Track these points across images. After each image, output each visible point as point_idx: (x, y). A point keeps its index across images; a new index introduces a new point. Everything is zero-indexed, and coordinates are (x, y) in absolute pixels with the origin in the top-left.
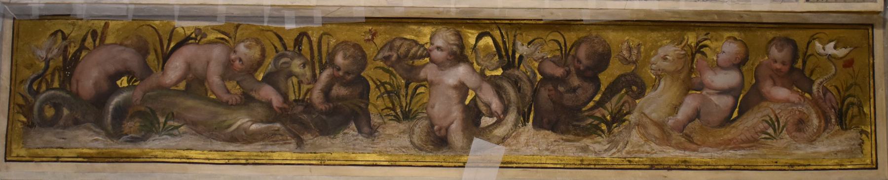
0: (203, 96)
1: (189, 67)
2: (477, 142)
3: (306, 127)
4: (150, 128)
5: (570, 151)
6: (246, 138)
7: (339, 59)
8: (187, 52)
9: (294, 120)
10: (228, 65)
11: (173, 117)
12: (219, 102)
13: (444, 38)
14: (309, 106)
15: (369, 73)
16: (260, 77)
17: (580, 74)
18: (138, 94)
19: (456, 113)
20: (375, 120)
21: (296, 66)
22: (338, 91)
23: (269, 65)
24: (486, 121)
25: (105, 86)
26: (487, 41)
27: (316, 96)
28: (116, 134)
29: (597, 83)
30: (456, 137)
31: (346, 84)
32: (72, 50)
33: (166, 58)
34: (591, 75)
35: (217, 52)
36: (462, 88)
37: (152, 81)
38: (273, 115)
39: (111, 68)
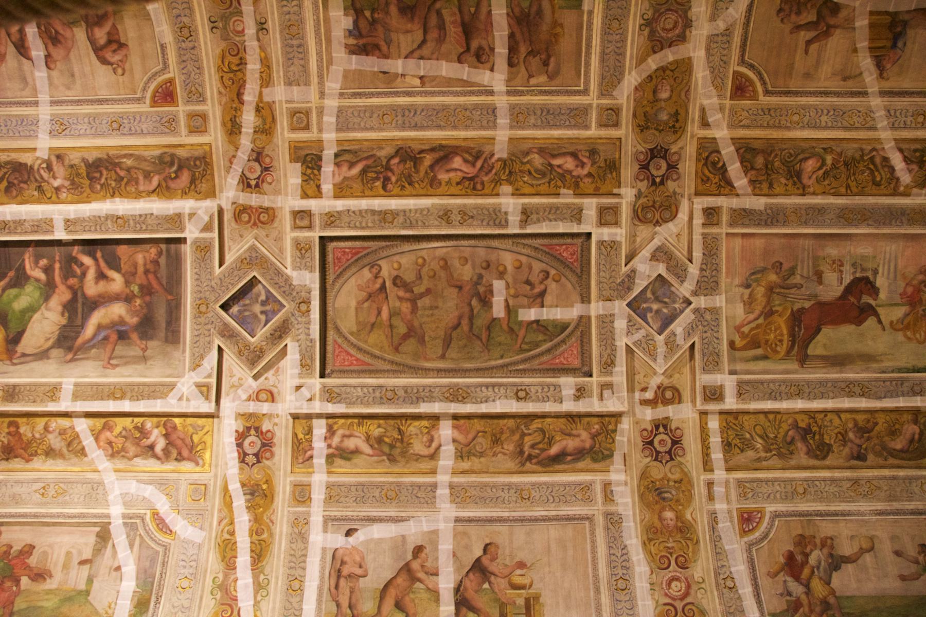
0: (144, 171)
1: (150, 181)
2: (46, 157)
3: (106, 160)
4: (161, 158)
5: (14, 156)
6: (125, 156)
7: (99, 187)
8: (152, 188)
9: (111, 163)
10: (137, 183)
11: (154, 163)
12: (138, 169)
13: (63, 196)
14: (107, 168)
15: (87, 182)
16: (125, 180)
17: (14, 185)
18: (167, 171)
19: (55, 168)
20: (83, 164)
21: (113, 184)
22: (97, 175)
23: (123, 183)
24: (44, 165)
25: (179, 174)
26: (49, 196)
27: (105, 172)
28: (173, 156)
29: (9, 183)
30: (54, 159)
31: (95, 177)
32: (193, 187)
33: (159, 185)
34: (10, 186)
35: (141, 188)
36: (55, 178)
37: (163, 176)
38: (118, 165)
39: (178, 181)
